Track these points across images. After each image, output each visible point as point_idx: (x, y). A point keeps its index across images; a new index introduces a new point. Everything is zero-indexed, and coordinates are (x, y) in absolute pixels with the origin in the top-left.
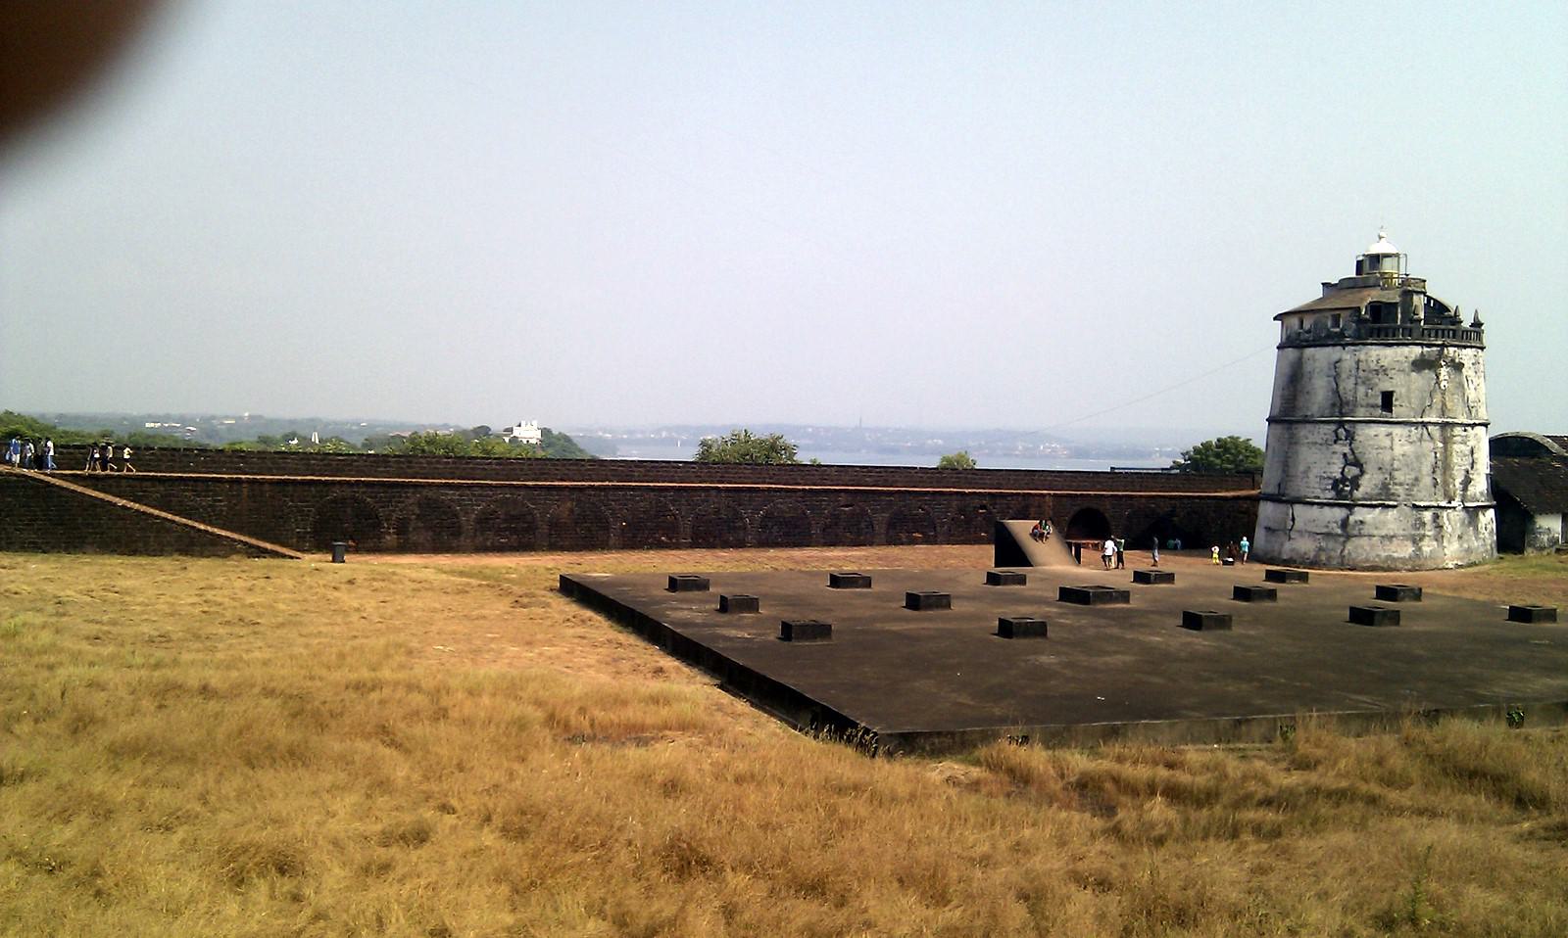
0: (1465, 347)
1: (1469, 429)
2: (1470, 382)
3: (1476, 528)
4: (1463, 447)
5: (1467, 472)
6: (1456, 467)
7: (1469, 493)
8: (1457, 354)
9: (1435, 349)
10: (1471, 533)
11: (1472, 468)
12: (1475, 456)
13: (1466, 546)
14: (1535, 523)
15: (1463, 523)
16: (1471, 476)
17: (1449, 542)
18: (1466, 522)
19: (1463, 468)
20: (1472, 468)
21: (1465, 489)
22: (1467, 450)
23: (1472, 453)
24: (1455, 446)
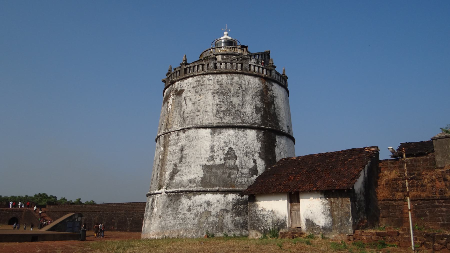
0: (186, 78)
1: (181, 133)
2: (188, 101)
3: (176, 210)
4: (174, 147)
5: (176, 165)
6: (169, 163)
7: (174, 181)
8: (180, 85)
9: (170, 87)
10: (169, 213)
11: (181, 161)
12: (185, 152)
13: (163, 223)
14: (256, 206)
15: (164, 205)
16: (179, 168)
17: (154, 221)
18: (167, 204)
19: (173, 162)
20: (181, 161)
21: (172, 178)
22: (177, 148)
23: (182, 150)
24: (170, 149)
